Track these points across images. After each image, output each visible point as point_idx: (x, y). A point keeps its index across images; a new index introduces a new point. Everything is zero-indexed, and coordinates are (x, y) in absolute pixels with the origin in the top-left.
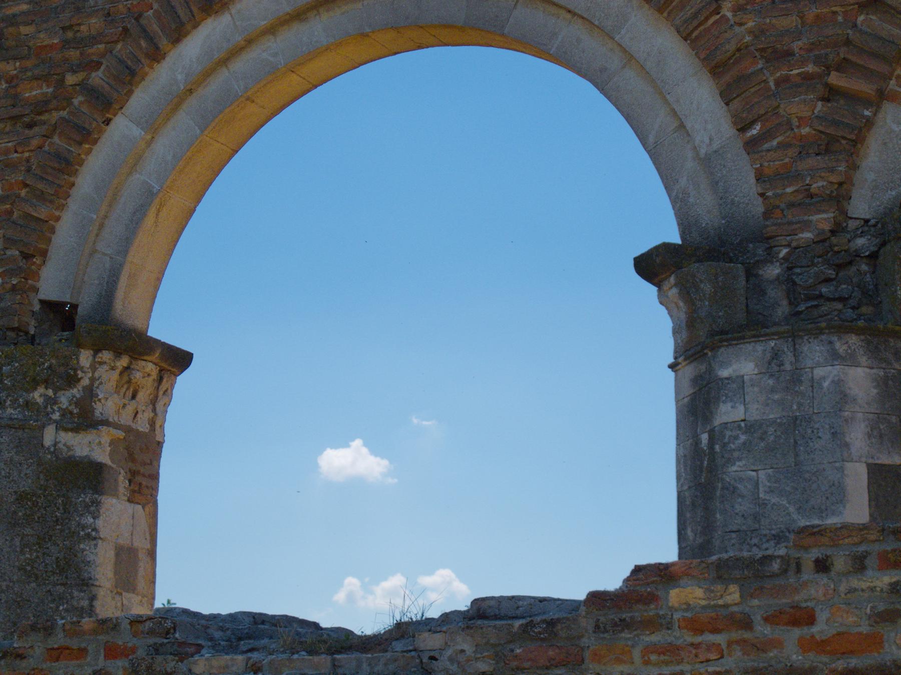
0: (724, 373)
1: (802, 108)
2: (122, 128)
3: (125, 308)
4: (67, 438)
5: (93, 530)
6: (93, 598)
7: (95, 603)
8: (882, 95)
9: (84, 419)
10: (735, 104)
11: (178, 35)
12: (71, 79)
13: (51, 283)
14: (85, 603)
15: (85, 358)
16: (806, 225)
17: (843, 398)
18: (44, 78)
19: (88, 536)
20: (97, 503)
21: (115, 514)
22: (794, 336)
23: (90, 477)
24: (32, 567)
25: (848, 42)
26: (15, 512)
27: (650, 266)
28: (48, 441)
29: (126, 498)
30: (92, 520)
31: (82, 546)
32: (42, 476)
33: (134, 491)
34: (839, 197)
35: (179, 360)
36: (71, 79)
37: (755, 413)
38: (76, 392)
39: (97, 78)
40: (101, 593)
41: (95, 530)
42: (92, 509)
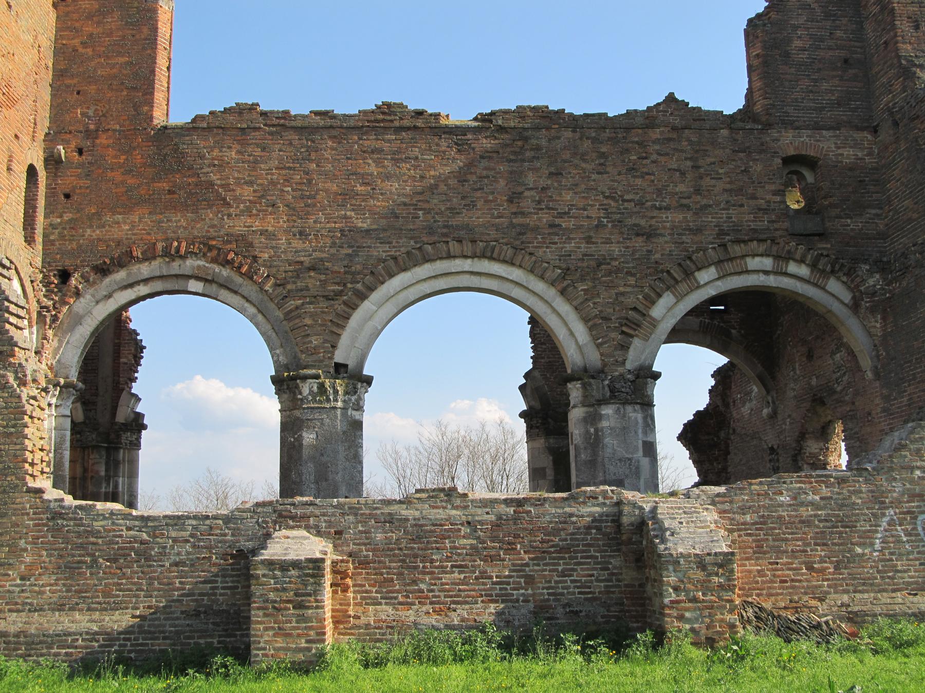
0: (603, 412)
2: (367, 306)
4: (354, 413)
10: (594, 333)
11: (391, 276)
12: (349, 285)
13: (339, 357)
15: (359, 385)
16: (616, 371)
18: (338, 284)
22: (624, 404)
25: (627, 319)
28: (349, 413)
36: (349, 285)
37: (612, 425)
38: (356, 397)
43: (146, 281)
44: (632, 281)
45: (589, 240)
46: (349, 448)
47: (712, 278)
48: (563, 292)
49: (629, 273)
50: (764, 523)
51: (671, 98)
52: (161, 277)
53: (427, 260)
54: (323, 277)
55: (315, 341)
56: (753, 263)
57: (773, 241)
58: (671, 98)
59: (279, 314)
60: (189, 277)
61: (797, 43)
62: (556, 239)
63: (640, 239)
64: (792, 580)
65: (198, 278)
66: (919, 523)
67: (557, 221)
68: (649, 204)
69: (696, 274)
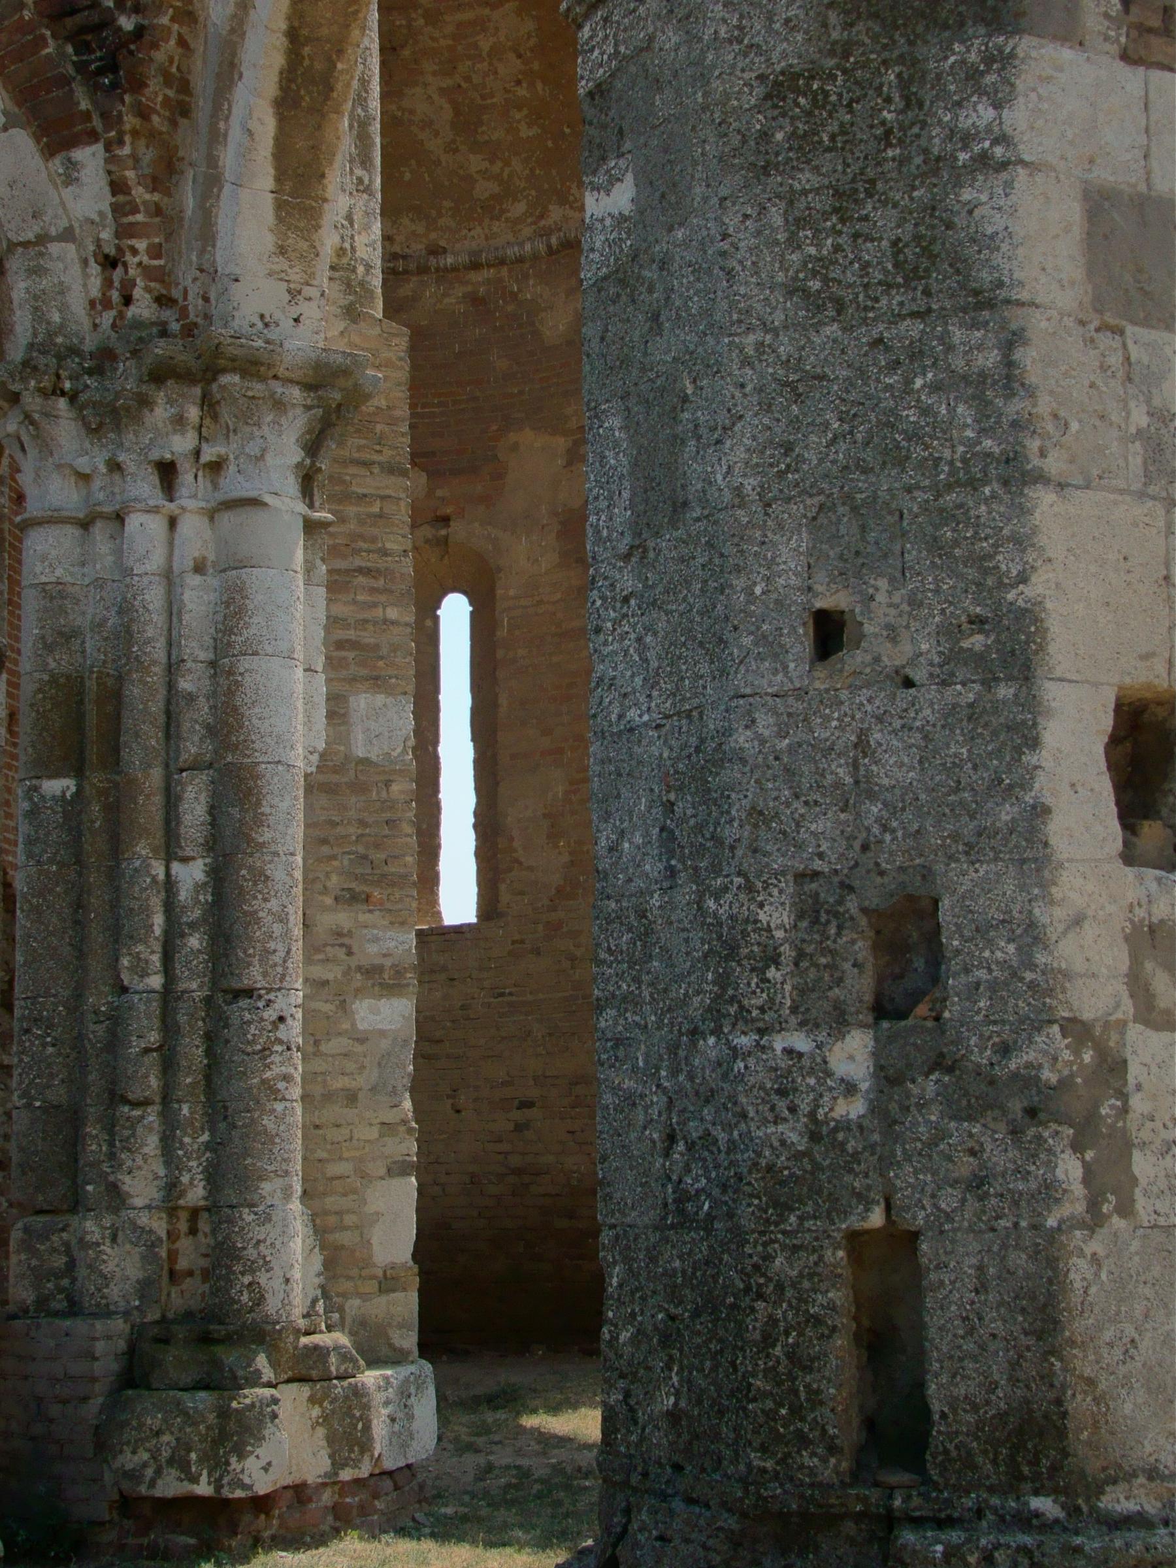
5: (996, 142)
6: (1012, 341)
7: (1017, 355)
14: (990, 359)
19: (983, 160)
20: (1002, 60)
24: (826, 280)
26: (765, 136)
29: (1114, 49)
30: (991, 113)
31: (967, 195)
32: (833, 17)
33: (1143, 30)
40: (1038, 324)
41: (1002, 139)
42: (990, 79)
46: (844, 202)
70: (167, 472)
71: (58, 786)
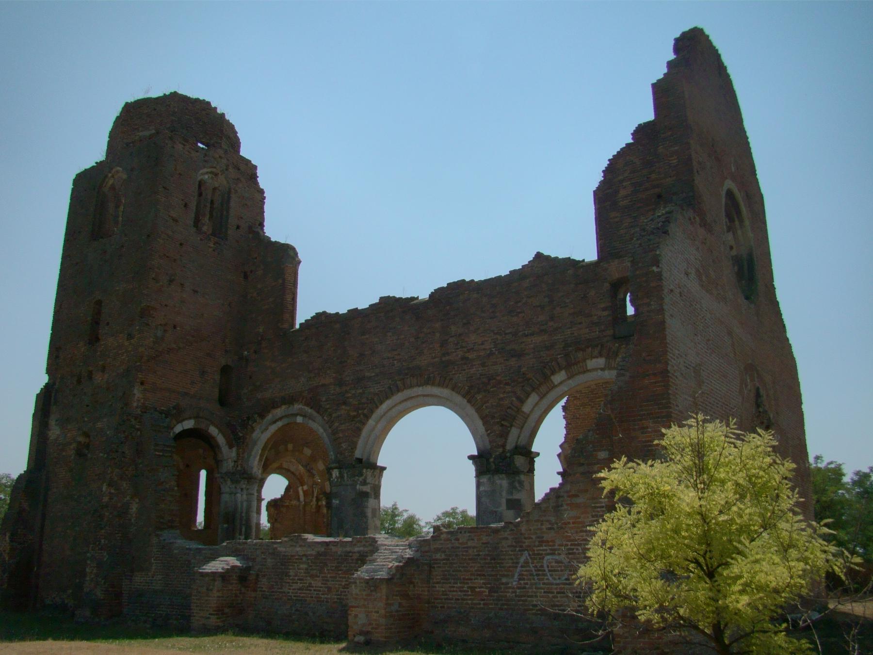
1: (497, 428)
2: (371, 422)
3: (372, 460)
4: (361, 487)
8: (511, 426)
9: (364, 483)
11: (381, 403)
13: (358, 454)
15: (364, 471)
17: (501, 486)
21: (371, 502)
23: (365, 495)
27: (471, 457)
34: (504, 446)
35: (383, 469)
39: (365, 411)
43: (280, 419)
44: (508, 388)
45: (483, 365)
47: (563, 379)
48: (469, 401)
49: (507, 384)
50: (448, 560)
51: (539, 256)
52: (286, 416)
53: (399, 390)
54: (348, 408)
55: (344, 446)
56: (591, 364)
57: (602, 346)
58: (539, 256)
59: (330, 431)
60: (296, 415)
61: (623, 193)
62: (465, 367)
63: (514, 359)
64: (463, 599)
65: (301, 415)
66: (545, 562)
67: (467, 355)
68: (521, 333)
69: (552, 377)
70: (242, 489)
71: (225, 526)
